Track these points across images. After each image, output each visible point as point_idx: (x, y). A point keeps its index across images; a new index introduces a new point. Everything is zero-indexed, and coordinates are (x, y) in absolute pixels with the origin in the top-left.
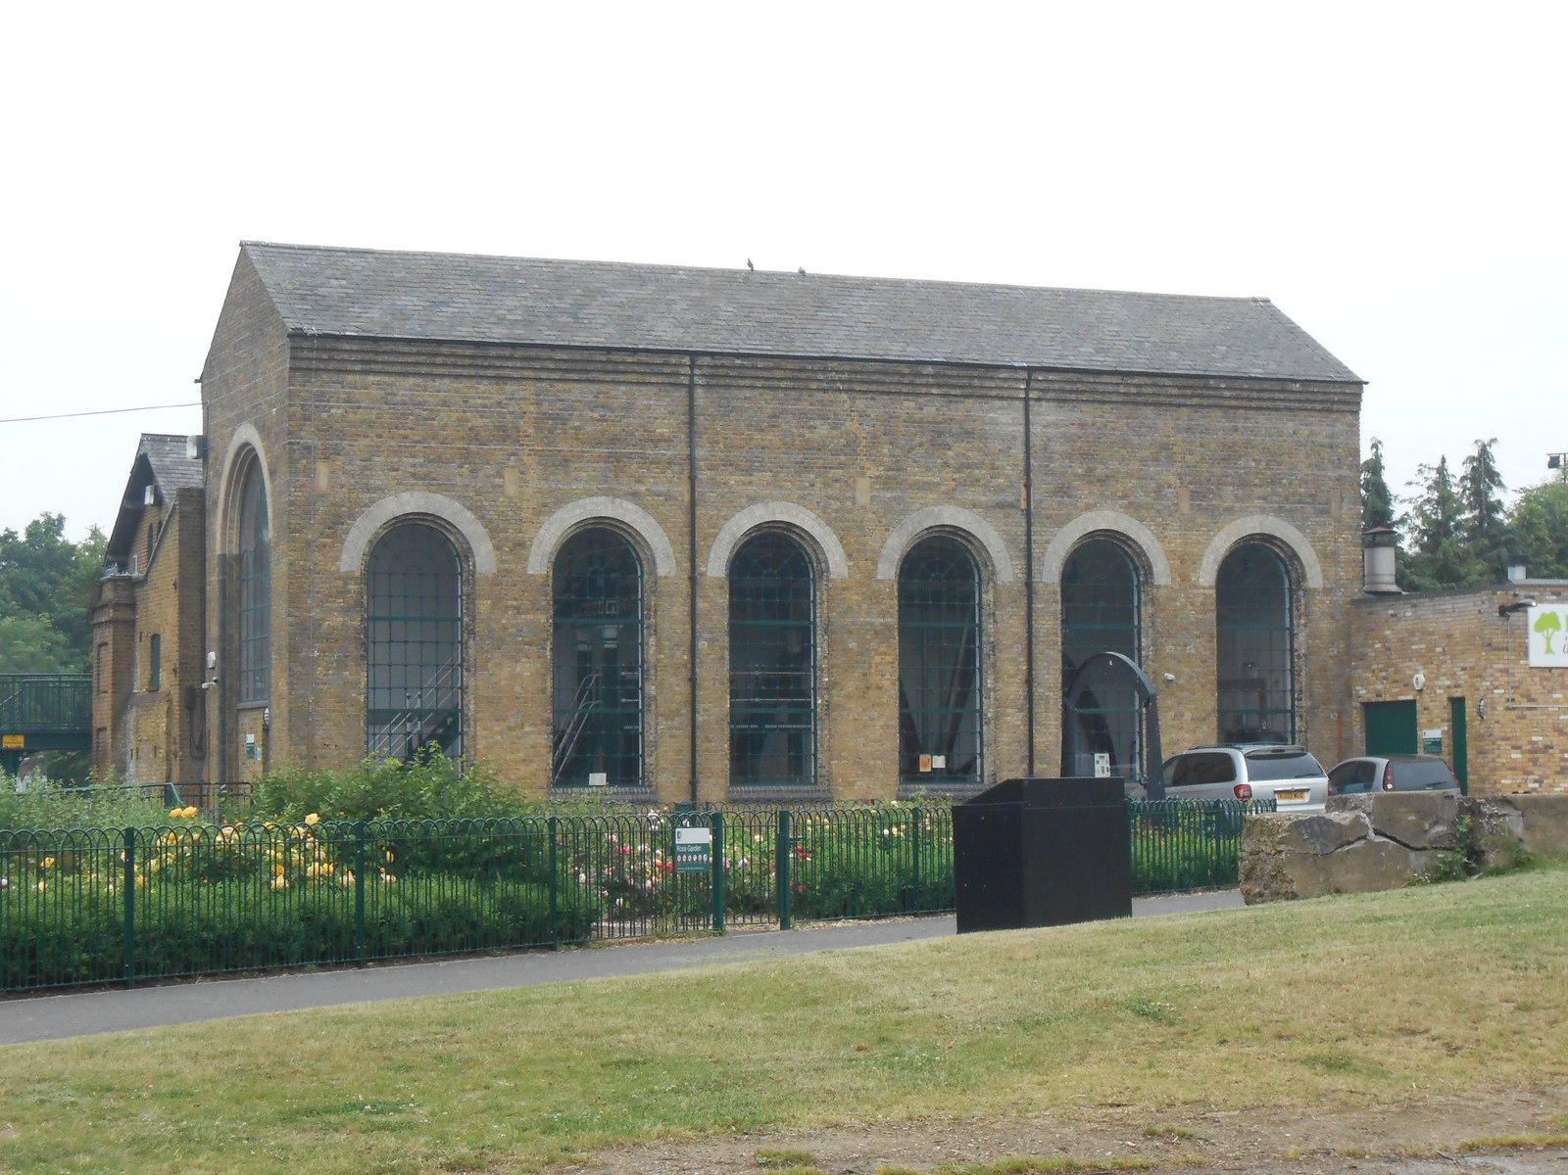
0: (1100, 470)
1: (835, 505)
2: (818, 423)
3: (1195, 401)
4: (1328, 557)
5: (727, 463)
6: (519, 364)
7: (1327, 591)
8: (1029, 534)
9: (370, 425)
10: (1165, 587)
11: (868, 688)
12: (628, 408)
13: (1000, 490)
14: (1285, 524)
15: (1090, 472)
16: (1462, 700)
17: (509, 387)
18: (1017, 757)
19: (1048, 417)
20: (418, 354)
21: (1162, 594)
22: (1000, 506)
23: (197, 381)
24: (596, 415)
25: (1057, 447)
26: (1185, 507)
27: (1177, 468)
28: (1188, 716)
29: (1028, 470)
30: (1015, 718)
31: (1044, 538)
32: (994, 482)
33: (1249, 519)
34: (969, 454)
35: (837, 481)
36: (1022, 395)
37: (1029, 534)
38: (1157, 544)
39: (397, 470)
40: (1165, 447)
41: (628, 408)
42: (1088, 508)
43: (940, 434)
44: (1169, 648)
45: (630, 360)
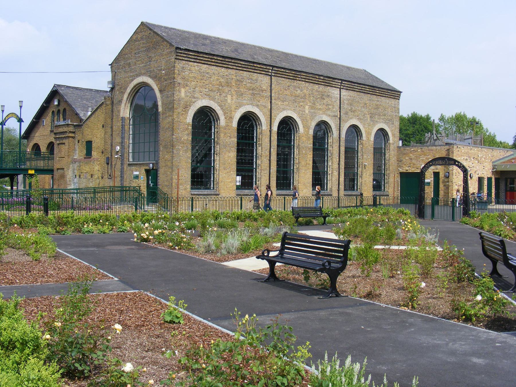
0: (353, 109)
2: (298, 89)
3: (371, 93)
4: (393, 135)
6: (232, 64)
7: (393, 144)
9: (195, 78)
12: (256, 80)
13: (334, 112)
16: (438, 173)
17: (230, 71)
19: (344, 92)
20: (208, 58)
21: (364, 142)
22: (334, 116)
23: (110, 65)
25: (345, 101)
30: (336, 173)
35: (302, 106)
39: (202, 92)
40: (366, 104)
41: (256, 80)
45: (258, 66)
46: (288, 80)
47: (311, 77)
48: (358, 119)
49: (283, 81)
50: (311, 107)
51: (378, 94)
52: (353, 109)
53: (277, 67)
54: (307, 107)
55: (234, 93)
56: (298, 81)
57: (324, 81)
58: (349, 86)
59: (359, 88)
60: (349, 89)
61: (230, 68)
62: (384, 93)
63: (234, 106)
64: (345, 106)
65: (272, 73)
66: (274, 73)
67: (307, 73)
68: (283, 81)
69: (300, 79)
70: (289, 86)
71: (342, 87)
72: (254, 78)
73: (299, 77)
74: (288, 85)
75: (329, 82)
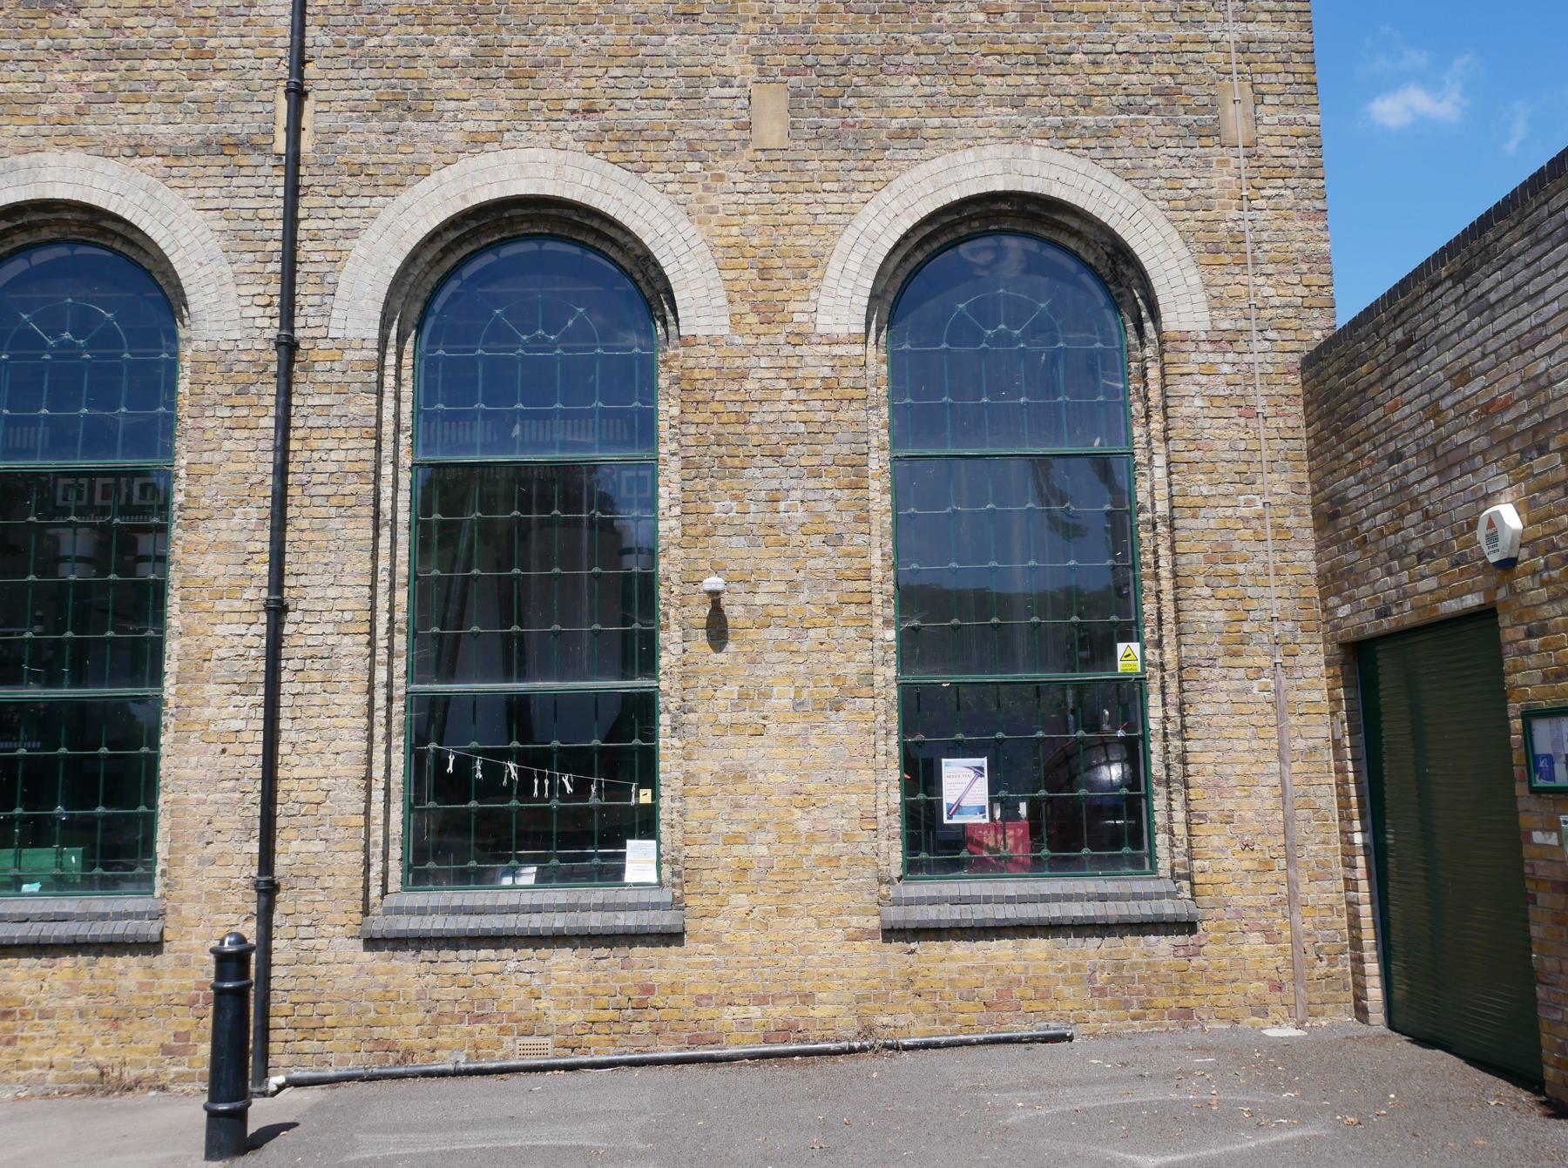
0: (514, 46)
7: (1222, 341)
8: (291, 220)
10: (712, 341)
14: (1084, 165)
15: (484, 56)
18: (227, 822)
26: (772, 129)
28: (783, 696)
29: (299, 60)
31: (339, 224)
32: (200, 90)
33: (970, 155)
34: (130, 22)
37: (291, 220)
38: (687, 228)
42: (476, 143)
44: (721, 507)
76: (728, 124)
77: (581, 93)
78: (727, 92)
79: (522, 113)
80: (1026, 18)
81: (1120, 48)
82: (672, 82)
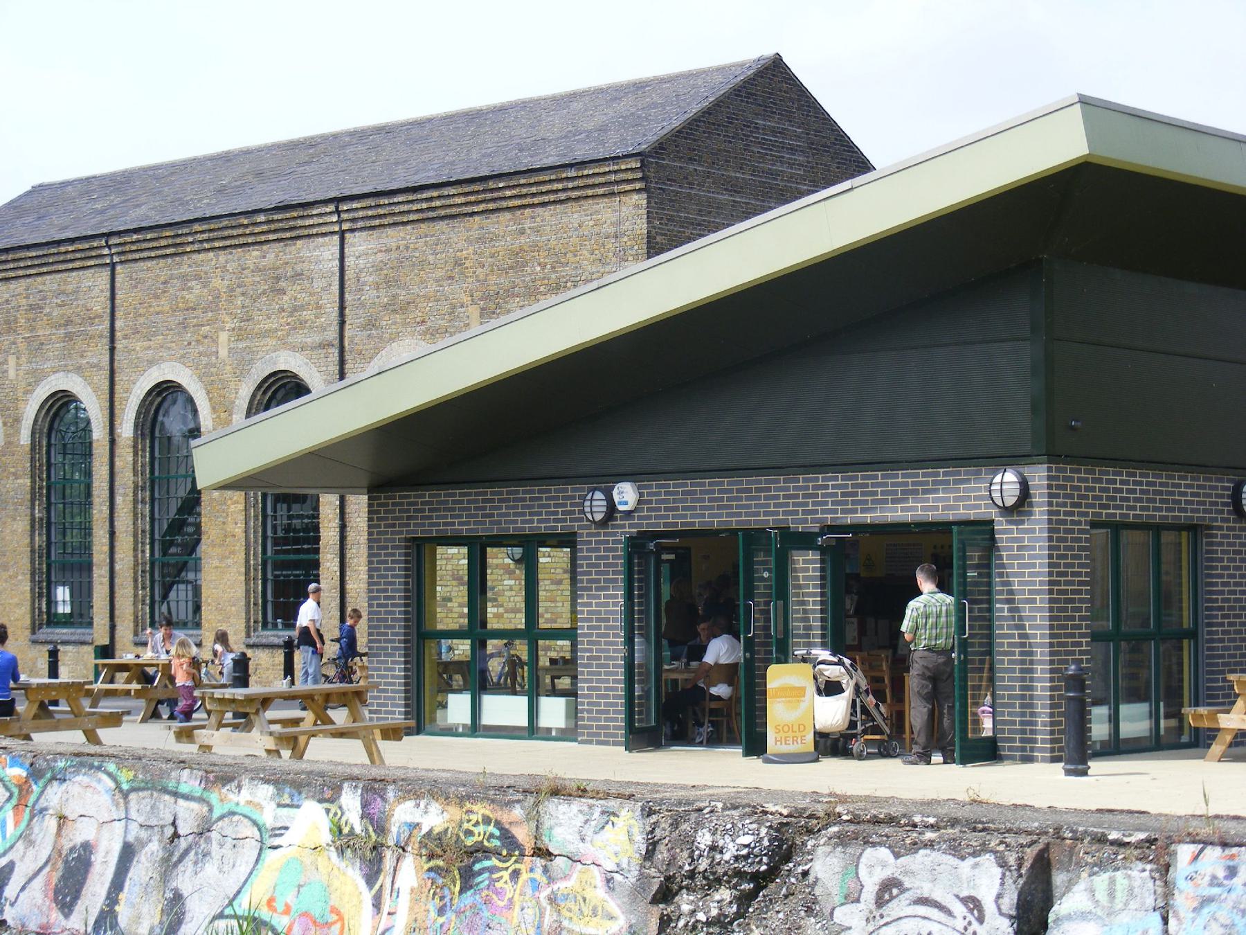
0: (403, 295)
1: (204, 360)
3: (482, 207)
5: (136, 332)
11: (225, 536)
17: (13, 285)
19: (359, 244)
22: (322, 346)
24: (59, 301)
25: (365, 278)
27: (470, 283)
35: (206, 337)
36: (337, 228)
40: (458, 263)
43: (278, 279)
45: (71, 248)
46: (162, 262)
47: (227, 228)
48: (424, 334)
49: (148, 269)
50: (240, 334)
51: (517, 202)
52: (403, 295)
53: (119, 233)
54: (223, 337)
55: (22, 346)
56: (195, 256)
57: (273, 227)
58: (370, 213)
59: (418, 206)
60: (377, 222)
61: (13, 278)
62: (544, 188)
63: (23, 384)
64: (365, 295)
65: (340, 222)
66: (119, 254)
67: (605, 159)
68: (148, 269)
69: (196, 247)
70: (165, 283)
71: (345, 226)
72: (70, 288)
73: (192, 243)
74: (162, 279)
75: (292, 223)
76: (462, 324)
77: (420, 314)
78: (463, 310)
79: (405, 324)
80: (553, 268)
81: (583, 278)
82: (446, 308)
